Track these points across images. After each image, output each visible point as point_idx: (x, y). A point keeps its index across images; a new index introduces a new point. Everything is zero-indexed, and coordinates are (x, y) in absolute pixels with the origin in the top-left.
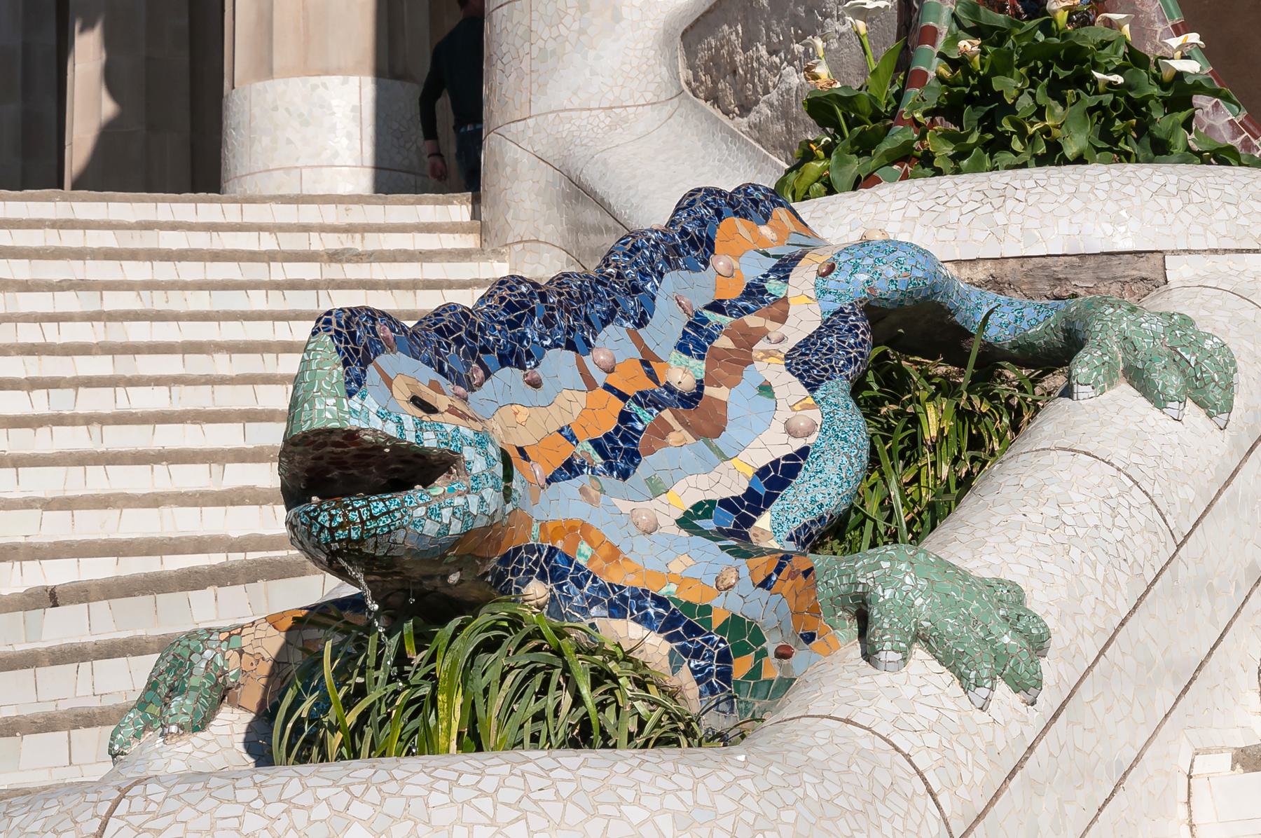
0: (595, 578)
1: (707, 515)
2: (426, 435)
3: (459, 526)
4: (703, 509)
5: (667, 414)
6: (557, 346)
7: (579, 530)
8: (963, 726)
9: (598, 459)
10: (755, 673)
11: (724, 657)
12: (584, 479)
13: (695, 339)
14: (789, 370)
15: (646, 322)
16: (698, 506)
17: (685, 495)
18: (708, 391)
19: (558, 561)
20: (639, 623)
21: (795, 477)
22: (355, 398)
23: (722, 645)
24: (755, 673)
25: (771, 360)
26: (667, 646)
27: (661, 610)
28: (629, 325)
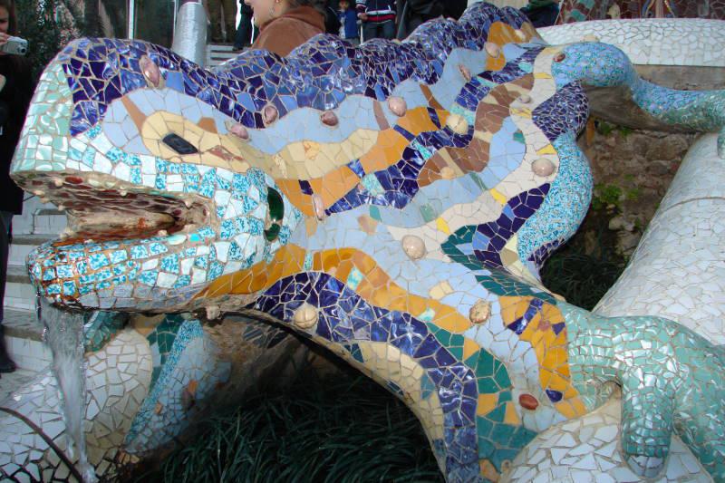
0: (362, 302)
2: (170, 179)
4: (464, 234)
5: (443, 152)
6: (357, 92)
9: (377, 190)
10: (499, 413)
12: (363, 210)
13: (470, 94)
14: (535, 123)
15: (435, 81)
16: (461, 231)
18: (477, 134)
19: (330, 287)
20: (398, 347)
21: (538, 207)
22: (81, 136)
23: (470, 378)
24: (499, 413)
25: (523, 114)
26: (419, 371)
27: (419, 335)
28: (422, 81)
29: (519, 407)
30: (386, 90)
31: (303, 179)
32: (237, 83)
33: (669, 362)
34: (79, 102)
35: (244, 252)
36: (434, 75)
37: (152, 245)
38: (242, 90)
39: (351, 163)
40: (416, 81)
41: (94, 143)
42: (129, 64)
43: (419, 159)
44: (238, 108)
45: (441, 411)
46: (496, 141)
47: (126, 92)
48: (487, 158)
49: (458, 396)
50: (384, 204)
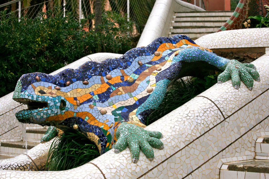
2: (39, 99)
3: (46, 116)
5: (120, 88)
7: (87, 114)
8: (126, 167)
11: (106, 143)
12: (91, 103)
14: (155, 77)
18: (136, 82)
23: (106, 140)
26: (98, 139)
31: (75, 97)
37: (35, 111)
38: (61, 79)
39: (91, 92)
40: (119, 69)
41: (25, 93)
43: (112, 90)
45: (100, 147)
46: (141, 84)
47: (32, 83)
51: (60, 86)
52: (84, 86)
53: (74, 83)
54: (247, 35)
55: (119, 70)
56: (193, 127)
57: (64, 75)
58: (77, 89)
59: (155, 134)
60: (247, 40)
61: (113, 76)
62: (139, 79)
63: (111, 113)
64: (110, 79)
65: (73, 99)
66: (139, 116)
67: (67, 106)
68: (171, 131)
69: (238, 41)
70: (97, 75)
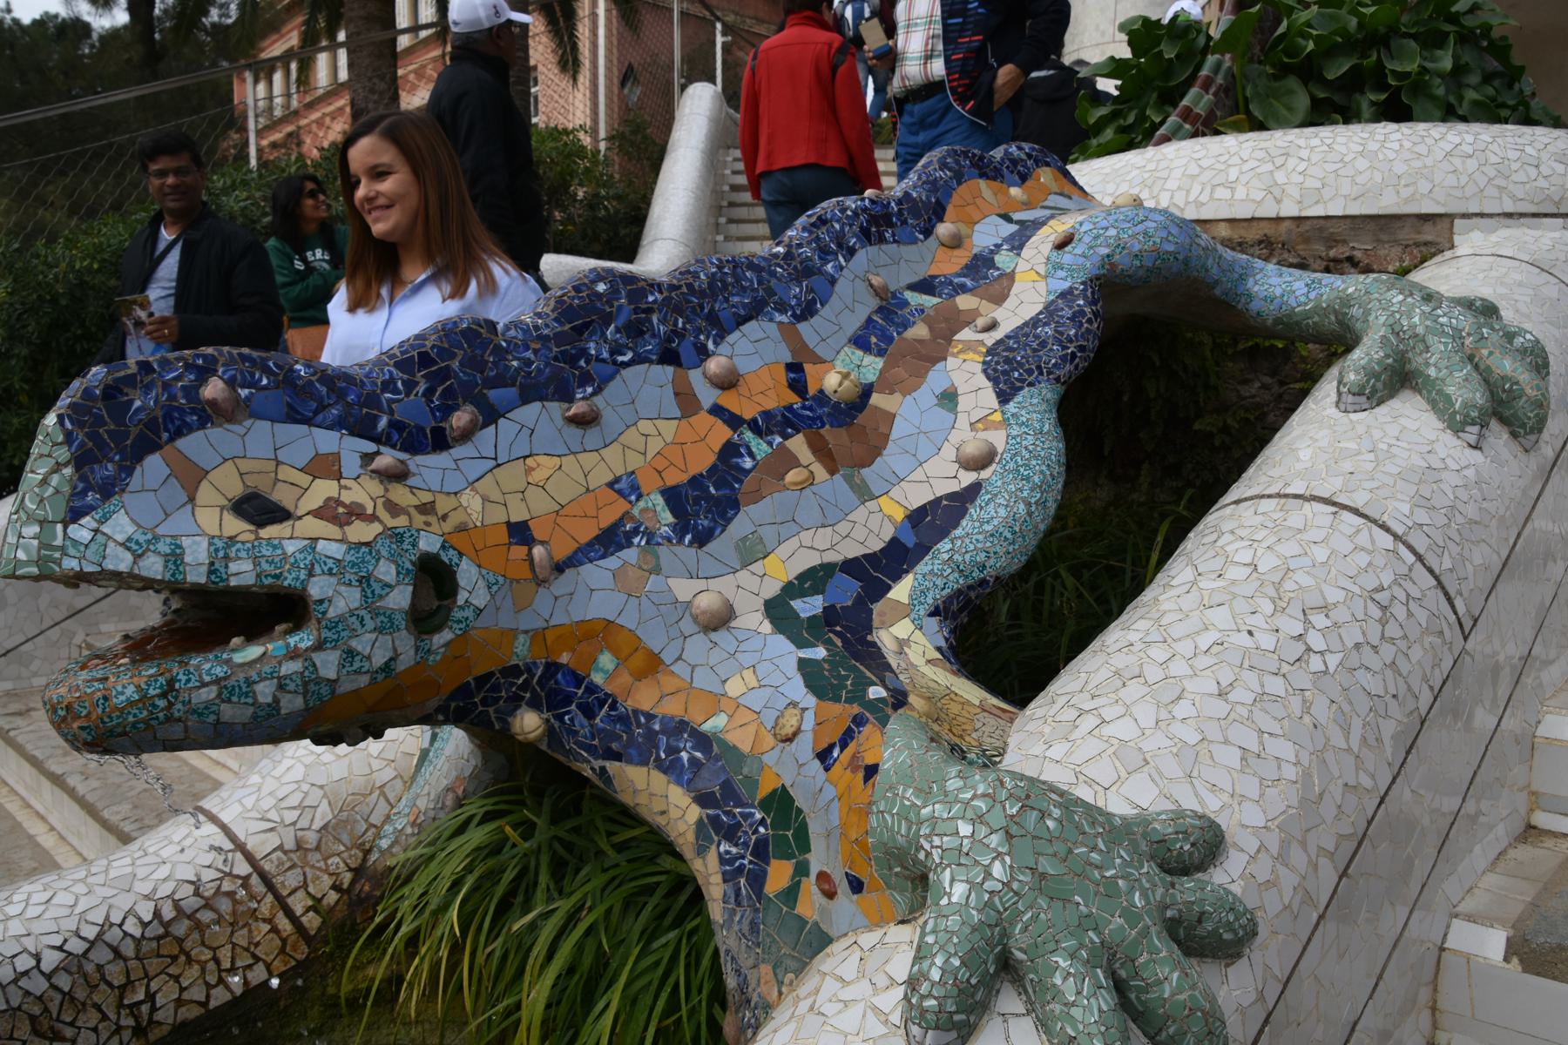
0: (615, 702)
1: (815, 591)
2: (234, 567)
4: (813, 580)
5: (798, 444)
7: (602, 633)
11: (761, 851)
12: (630, 555)
14: (985, 371)
17: (782, 566)
18: (876, 399)
20: (665, 772)
21: (956, 525)
22: (86, 520)
23: (762, 830)
26: (695, 812)
27: (698, 755)
29: (814, 889)
30: (704, 347)
31: (514, 519)
32: (399, 384)
33: (997, 864)
34: (86, 469)
35: (369, 658)
36: (814, 301)
37: (207, 666)
38: (408, 395)
39: (617, 480)
40: (771, 320)
41: (105, 529)
42: (180, 394)
43: (748, 459)
44: (393, 424)
46: (908, 412)
47: (172, 440)
48: (886, 438)
49: (743, 857)
50: (669, 540)
51: (404, 449)
52: (574, 432)
53: (501, 421)
54: (1352, 156)
55: (774, 326)
56: (1357, 724)
57: (434, 362)
58: (529, 461)
59: (1187, 847)
60: (1359, 179)
61: (744, 366)
62: (886, 383)
63: (759, 616)
64: (728, 382)
65: (503, 536)
66: (934, 621)
67: (462, 597)
68: (1251, 787)
69: (1307, 185)
70: (651, 362)
